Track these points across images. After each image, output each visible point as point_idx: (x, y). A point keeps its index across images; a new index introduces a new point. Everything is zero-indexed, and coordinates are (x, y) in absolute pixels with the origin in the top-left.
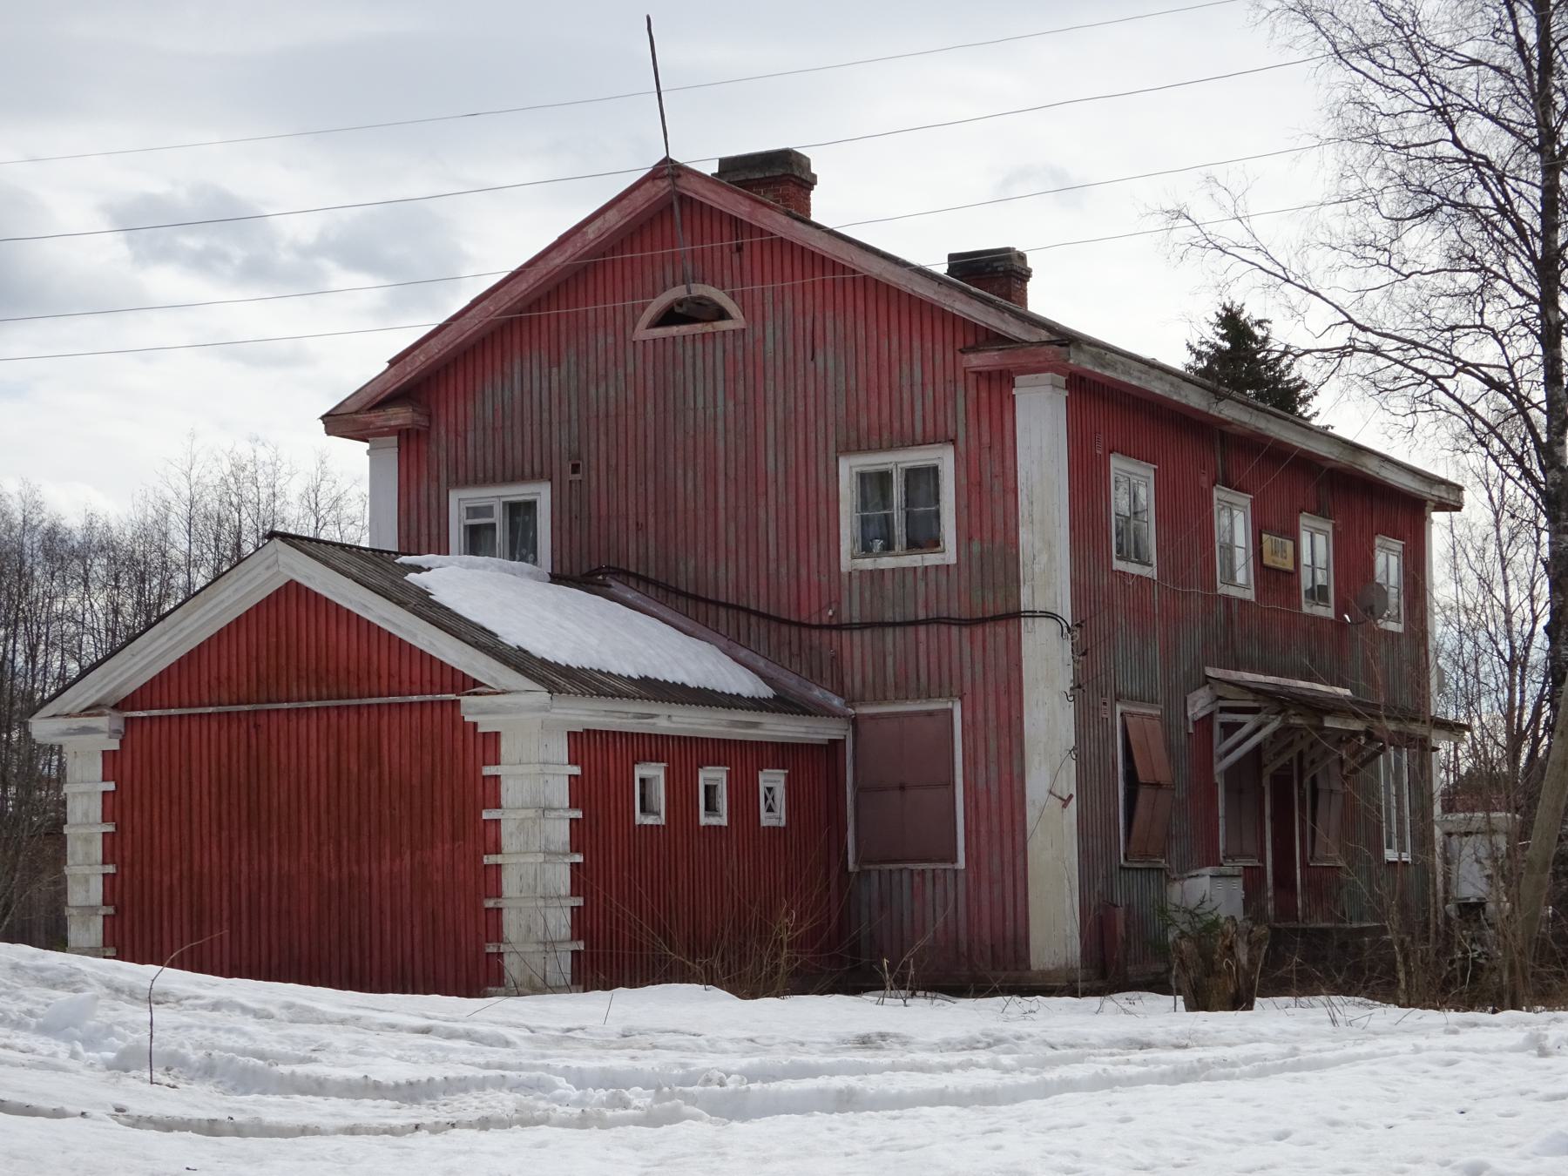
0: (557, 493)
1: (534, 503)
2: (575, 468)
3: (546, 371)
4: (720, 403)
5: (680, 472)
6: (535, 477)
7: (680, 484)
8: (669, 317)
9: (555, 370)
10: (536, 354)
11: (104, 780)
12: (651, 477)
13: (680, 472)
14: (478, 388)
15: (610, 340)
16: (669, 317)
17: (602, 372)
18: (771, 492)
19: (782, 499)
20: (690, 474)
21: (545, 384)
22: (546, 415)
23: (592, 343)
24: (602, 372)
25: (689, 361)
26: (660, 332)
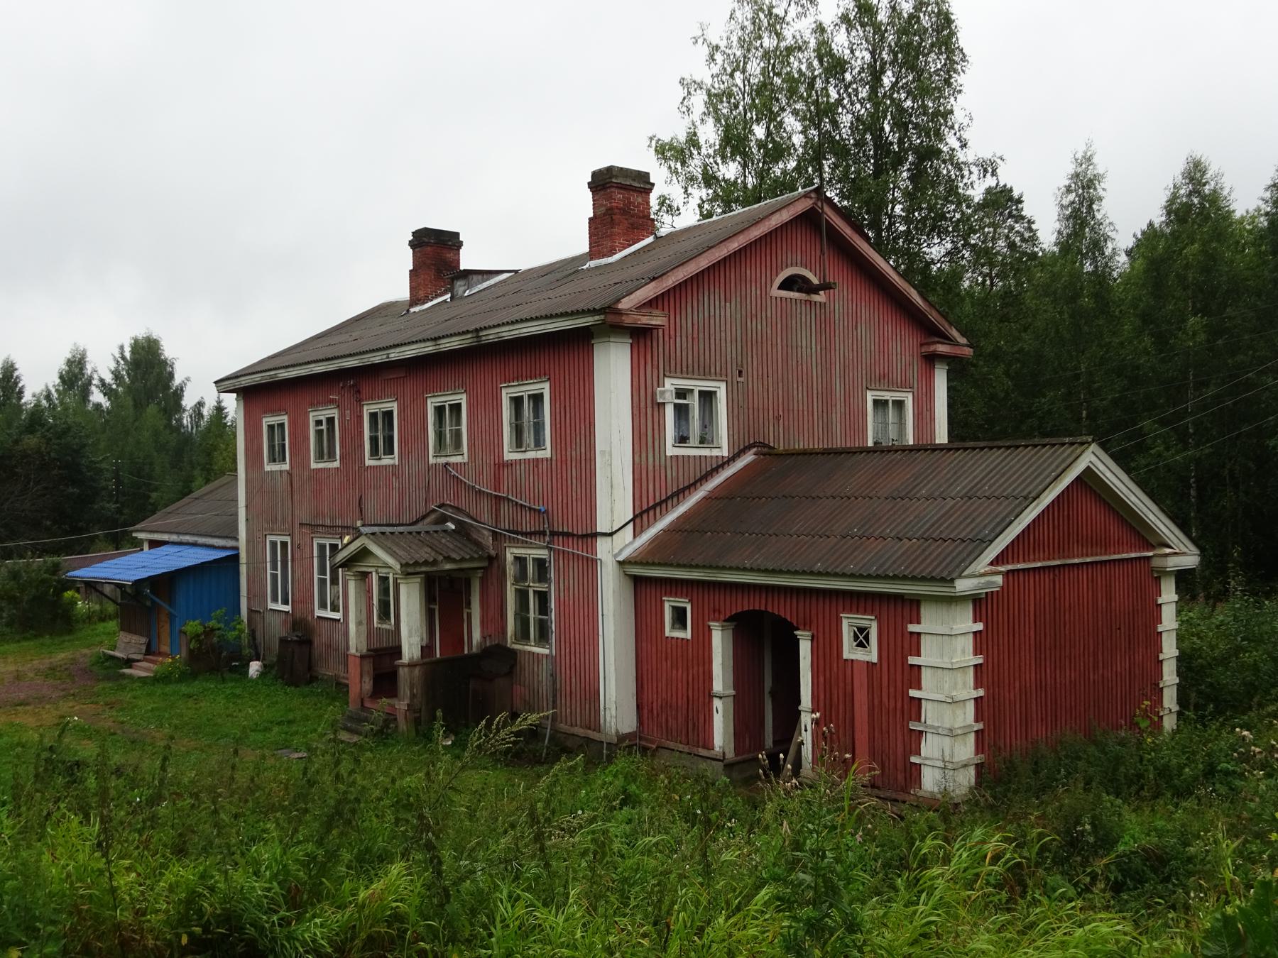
0: (730, 389)
1: (715, 392)
2: (740, 372)
3: (723, 303)
4: (814, 346)
5: (795, 386)
6: (718, 376)
7: (795, 392)
8: (788, 284)
9: (728, 304)
10: (717, 290)
11: (975, 621)
12: (780, 385)
13: (795, 386)
14: (683, 306)
15: (759, 292)
16: (788, 284)
17: (754, 312)
18: (838, 407)
19: (843, 410)
20: (800, 388)
21: (723, 314)
22: (723, 334)
23: (748, 291)
24: (754, 312)
25: (799, 316)
26: (784, 293)
